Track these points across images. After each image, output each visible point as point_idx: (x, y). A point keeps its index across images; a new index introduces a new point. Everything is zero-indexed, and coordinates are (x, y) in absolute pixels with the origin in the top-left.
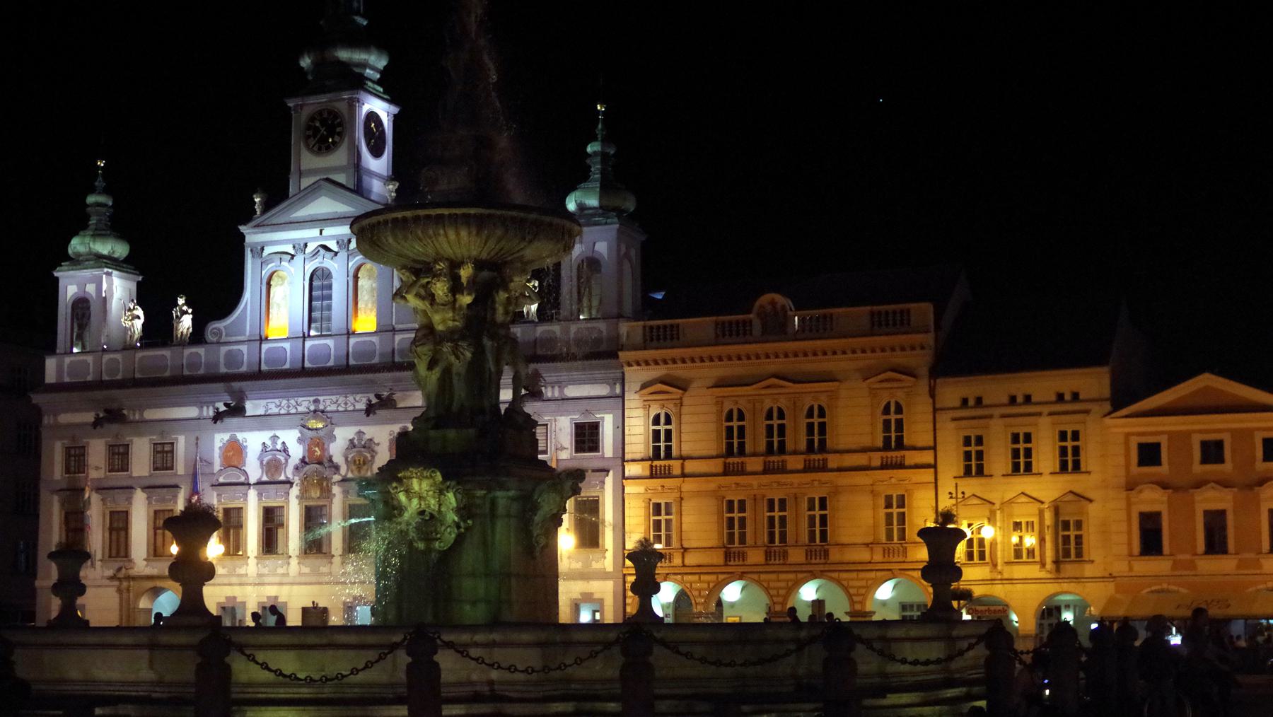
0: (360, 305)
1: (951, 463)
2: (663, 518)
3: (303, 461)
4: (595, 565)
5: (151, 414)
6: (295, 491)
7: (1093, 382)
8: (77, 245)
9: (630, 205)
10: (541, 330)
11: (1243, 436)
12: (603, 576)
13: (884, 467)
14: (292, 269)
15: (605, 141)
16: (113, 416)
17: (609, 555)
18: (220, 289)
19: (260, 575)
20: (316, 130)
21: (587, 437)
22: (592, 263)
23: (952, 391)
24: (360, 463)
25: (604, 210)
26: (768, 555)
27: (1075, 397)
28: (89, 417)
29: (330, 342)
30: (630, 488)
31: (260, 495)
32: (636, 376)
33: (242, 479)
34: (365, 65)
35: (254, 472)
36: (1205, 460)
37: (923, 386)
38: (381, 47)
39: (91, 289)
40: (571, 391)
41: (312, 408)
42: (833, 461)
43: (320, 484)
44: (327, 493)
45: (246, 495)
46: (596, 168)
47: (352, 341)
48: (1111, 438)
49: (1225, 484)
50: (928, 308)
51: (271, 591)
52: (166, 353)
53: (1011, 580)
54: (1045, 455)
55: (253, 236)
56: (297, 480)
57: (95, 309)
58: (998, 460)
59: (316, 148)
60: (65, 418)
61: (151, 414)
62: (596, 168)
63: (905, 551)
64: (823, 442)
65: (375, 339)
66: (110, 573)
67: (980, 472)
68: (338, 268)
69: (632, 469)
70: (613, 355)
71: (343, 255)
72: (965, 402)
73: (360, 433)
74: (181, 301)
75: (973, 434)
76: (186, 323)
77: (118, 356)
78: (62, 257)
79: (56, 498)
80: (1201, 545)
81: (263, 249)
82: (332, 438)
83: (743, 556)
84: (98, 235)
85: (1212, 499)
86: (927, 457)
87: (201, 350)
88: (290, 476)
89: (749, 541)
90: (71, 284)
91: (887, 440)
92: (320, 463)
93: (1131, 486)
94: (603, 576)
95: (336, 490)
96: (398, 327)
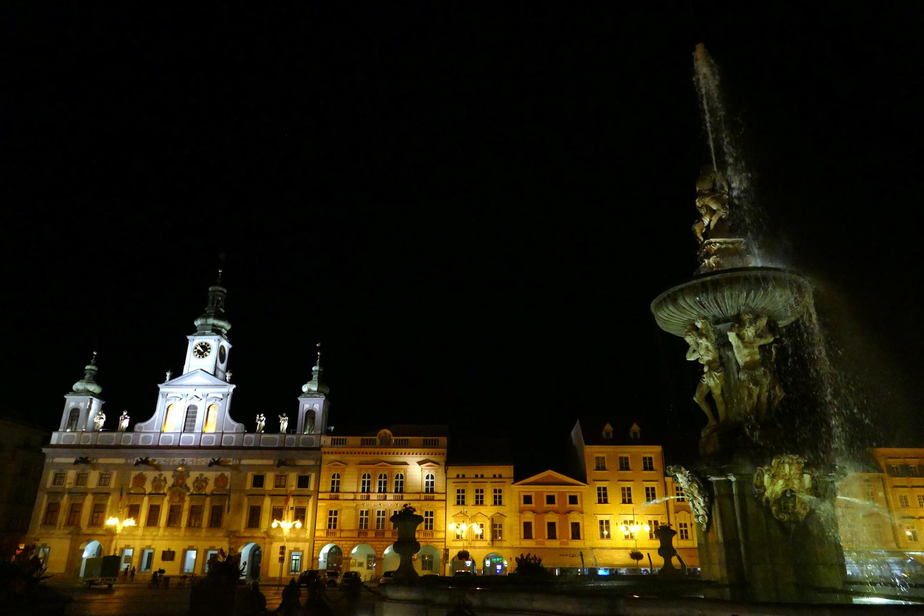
1: (452, 498)
2: (333, 517)
3: (173, 485)
4: (302, 536)
5: (101, 461)
6: (167, 498)
7: (507, 471)
8: (78, 386)
9: (327, 391)
10: (288, 436)
11: (562, 494)
12: (305, 540)
13: (426, 500)
15: (320, 366)
16: (83, 461)
17: (308, 532)
18: (144, 409)
20: (199, 351)
22: (310, 414)
23: (454, 471)
24: (199, 488)
25: (319, 392)
26: (376, 534)
27: (500, 476)
28: (72, 460)
29: (193, 435)
30: (320, 504)
31: (150, 500)
34: (222, 327)
35: (148, 488)
36: (571, 503)
38: (230, 322)
39: (82, 405)
42: (406, 497)
43: (180, 495)
44: (182, 500)
45: (142, 499)
46: (315, 376)
48: (513, 493)
49: (556, 512)
51: (148, 543)
52: (114, 435)
53: (474, 547)
54: (489, 498)
55: (163, 388)
56: (169, 494)
57: (82, 414)
58: (470, 498)
60: (57, 460)
61: (101, 461)
62: (315, 376)
63: (433, 534)
64: (401, 489)
65: (214, 436)
66: (66, 532)
67: (463, 503)
69: (321, 496)
70: (319, 449)
71: (204, 400)
72: (458, 476)
73: (201, 475)
74: (125, 413)
75: (461, 488)
76: (125, 423)
77: (90, 435)
78: (69, 390)
79: (46, 497)
80: (546, 537)
82: (189, 476)
83: (366, 534)
84: (89, 382)
85: (551, 518)
86: (443, 497)
87: (131, 435)
89: (369, 527)
90: (71, 402)
91: (427, 489)
92: (181, 486)
93: (521, 511)
94: (305, 540)
95: (187, 499)
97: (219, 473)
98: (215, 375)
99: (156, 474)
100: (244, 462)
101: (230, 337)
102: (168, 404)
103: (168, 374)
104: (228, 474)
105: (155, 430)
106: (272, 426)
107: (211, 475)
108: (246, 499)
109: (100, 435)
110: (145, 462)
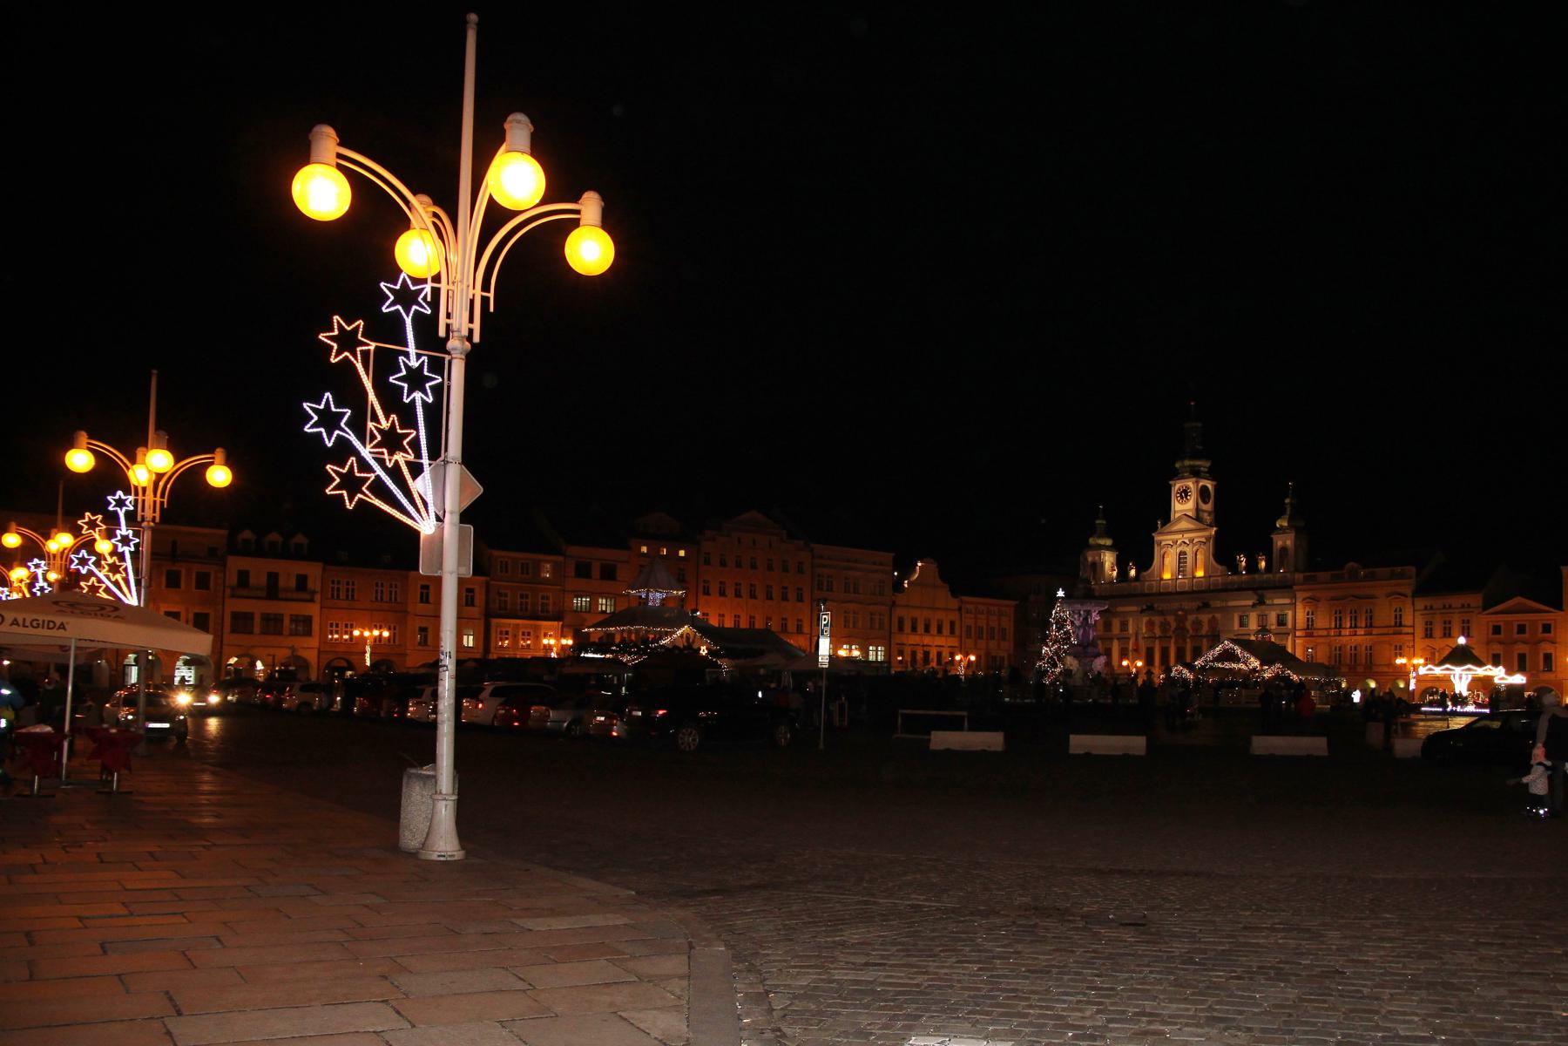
21: (1281, 622)
22: (1284, 549)
24: (1196, 630)
32: (1300, 595)
35: (1158, 632)
37: (1409, 600)
40: (1277, 601)
42: (1375, 631)
50: (1413, 569)
55: (1157, 538)
68: (1188, 549)
76: (1133, 573)
84: (1101, 537)
98: (1198, 519)
100: (1231, 604)
101: (1211, 475)
104: (1218, 616)
106: (1252, 567)
107: (1205, 618)
110: (1150, 608)
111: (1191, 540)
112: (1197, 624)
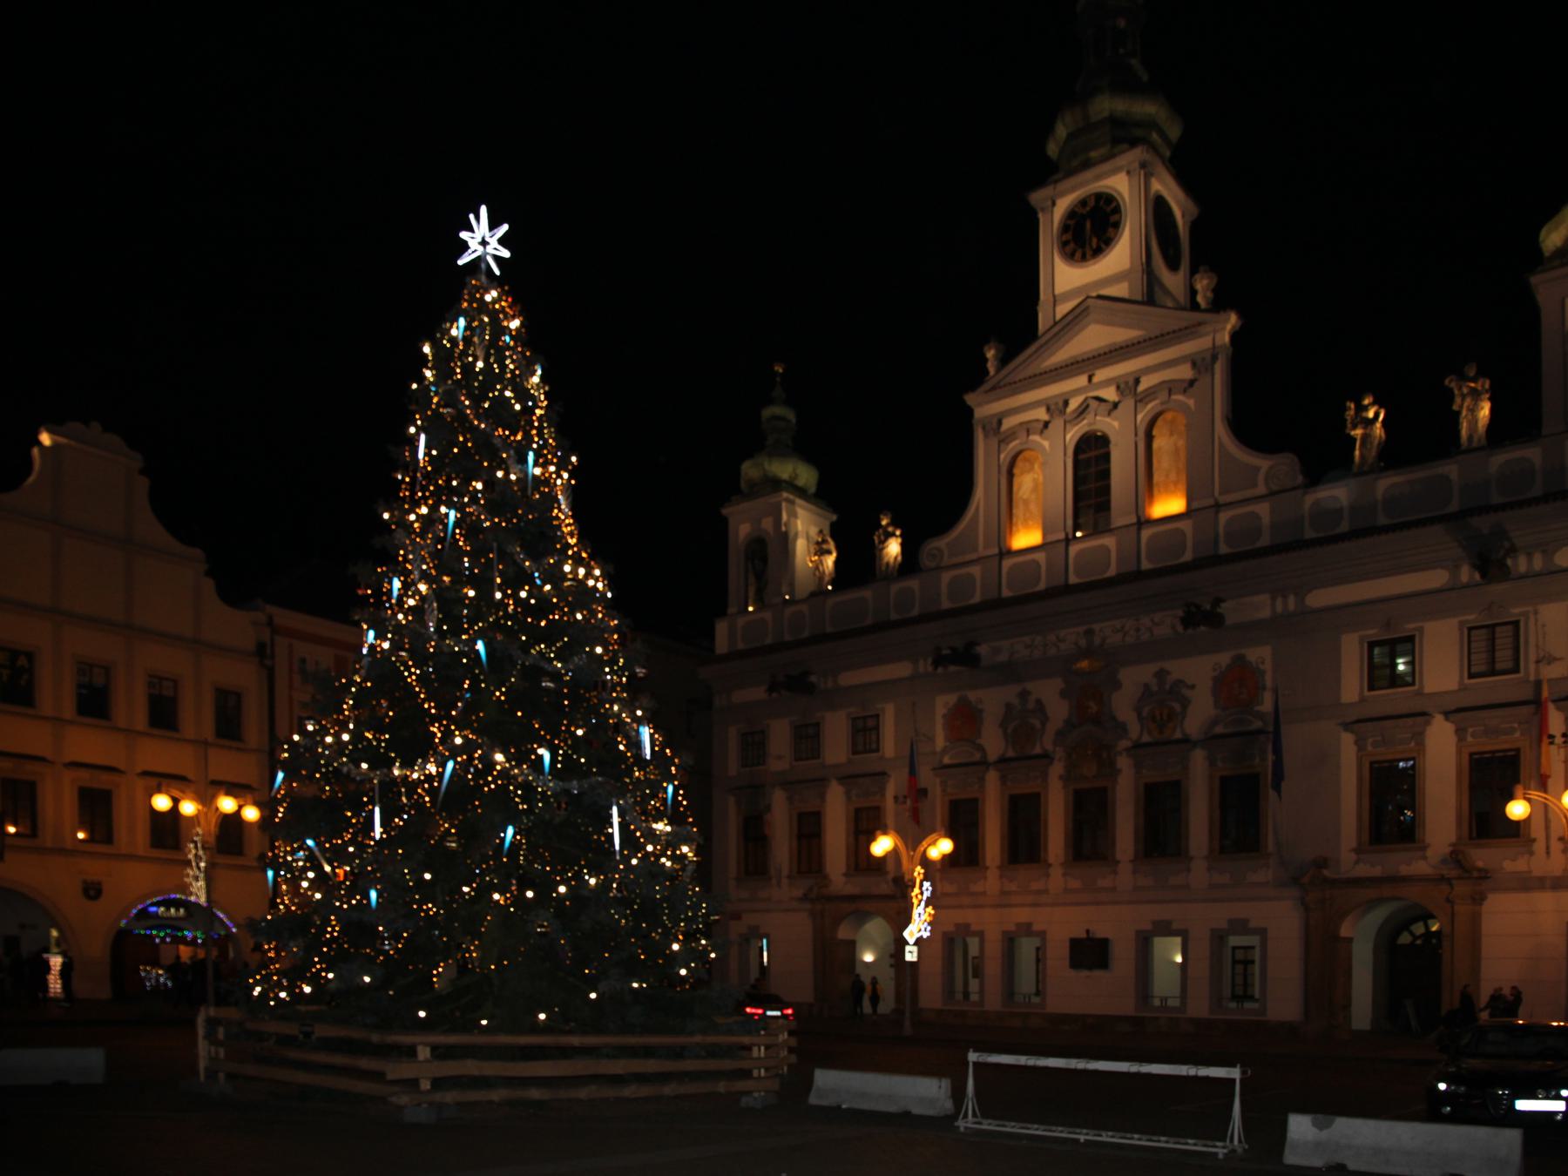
0: (1156, 478)
14: (1046, 444)
19: (1003, 893)
29: (1109, 541)
31: (1003, 779)
33: (977, 756)
35: (993, 742)
41: (1083, 643)
47: (1146, 534)
55: (984, 408)
59: (1078, 255)
65: (1186, 526)
68: (1118, 428)
73: (1161, 675)
76: (893, 548)
81: (1000, 423)
82: (1117, 685)
88: (1049, 747)
95: (1124, 763)
96: (1222, 500)
97: (1224, 659)
99: (1009, 693)
100: (1319, 599)
102: (1004, 457)
103: (990, 354)
105: (982, 552)
108: (1347, 739)
109: (830, 602)
110: (966, 657)
111: (1128, 386)
112: (1164, 703)
